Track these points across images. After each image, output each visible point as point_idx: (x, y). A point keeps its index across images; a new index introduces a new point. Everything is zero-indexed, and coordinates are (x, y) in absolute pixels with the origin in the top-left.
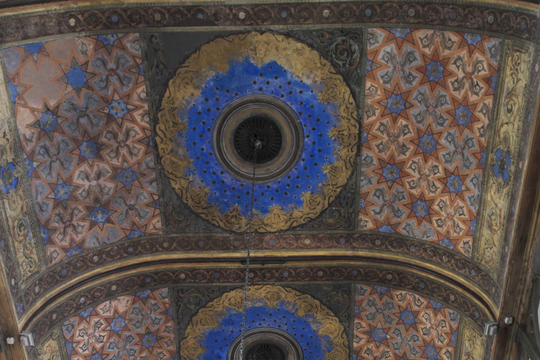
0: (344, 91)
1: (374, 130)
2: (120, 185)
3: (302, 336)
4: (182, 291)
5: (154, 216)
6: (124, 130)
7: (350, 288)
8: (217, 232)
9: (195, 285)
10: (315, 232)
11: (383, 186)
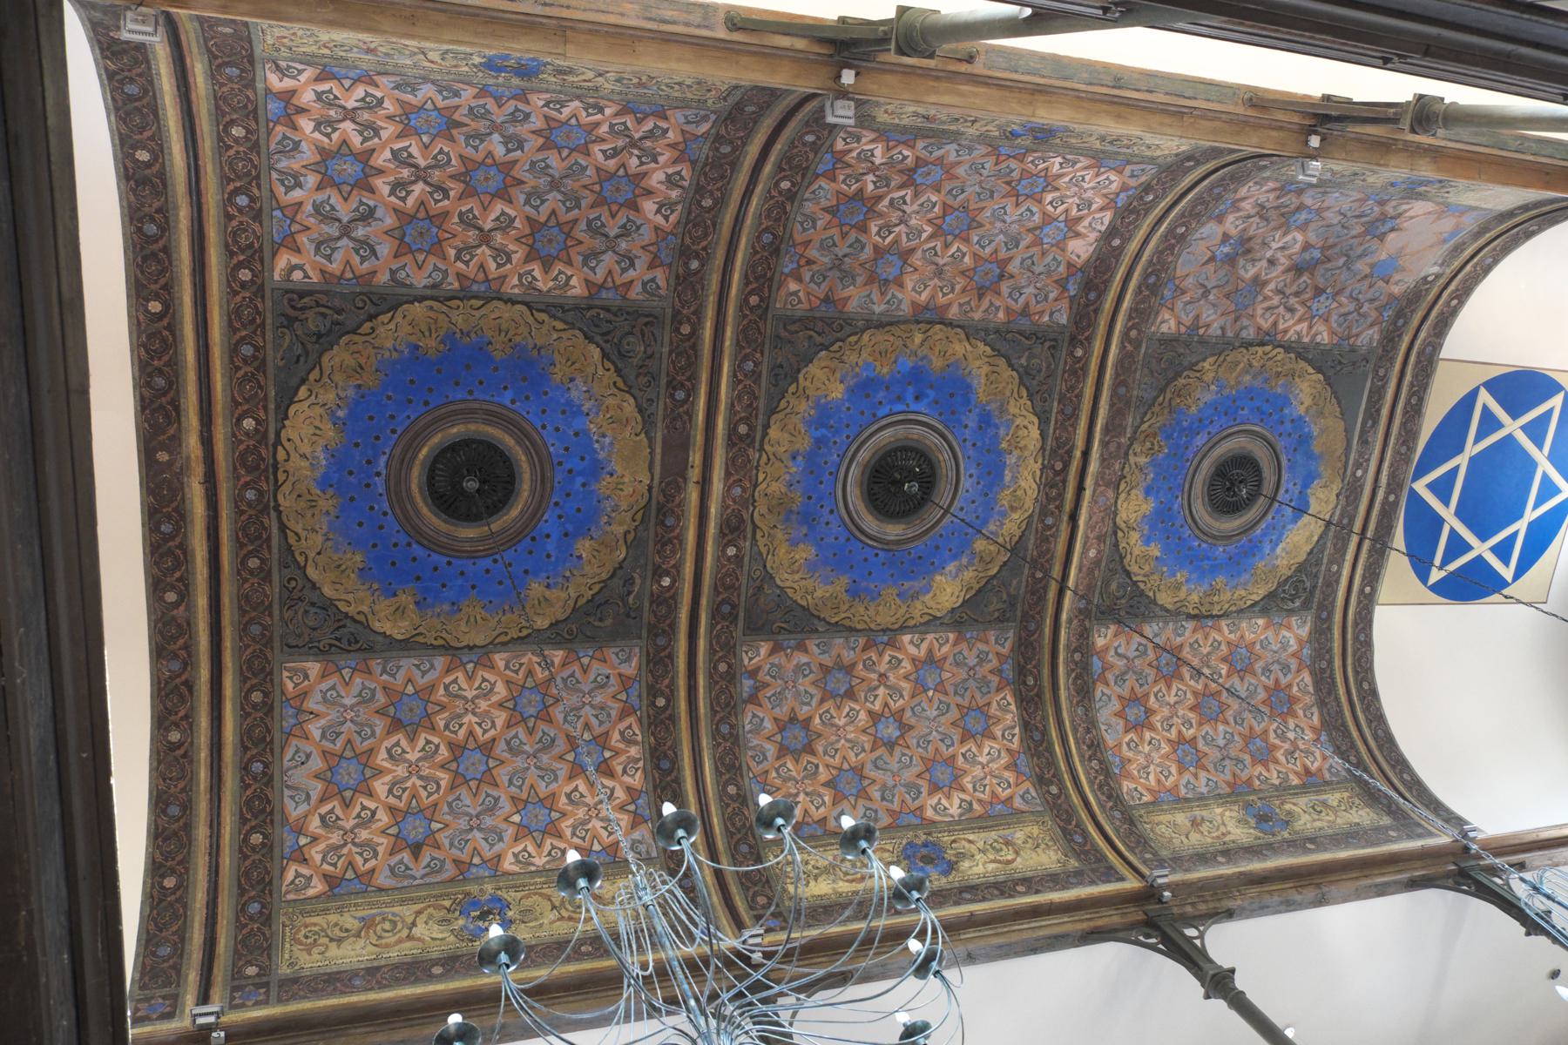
0: (1259, 592)
1: (1214, 635)
2: (1242, 285)
3: (937, 547)
4: (1054, 347)
7: (1008, 620)
9: (1060, 372)
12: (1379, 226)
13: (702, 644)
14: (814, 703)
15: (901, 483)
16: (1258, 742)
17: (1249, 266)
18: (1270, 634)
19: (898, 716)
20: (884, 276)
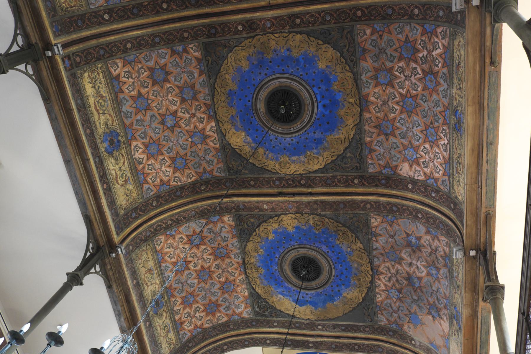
0: (259, 290)
1: (237, 273)
2: (398, 253)
3: (257, 130)
4: (357, 168)
5: (376, 227)
6: (392, 282)
7: (229, 172)
8: (330, 214)
9: (346, 174)
10: (261, 213)
11: (224, 244)
12: (434, 310)
13: (195, 22)
14: (176, 83)
15: (284, 106)
16: (192, 299)
17: (407, 254)
18: (242, 299)
19: (177, 125)
20: (379, 76)
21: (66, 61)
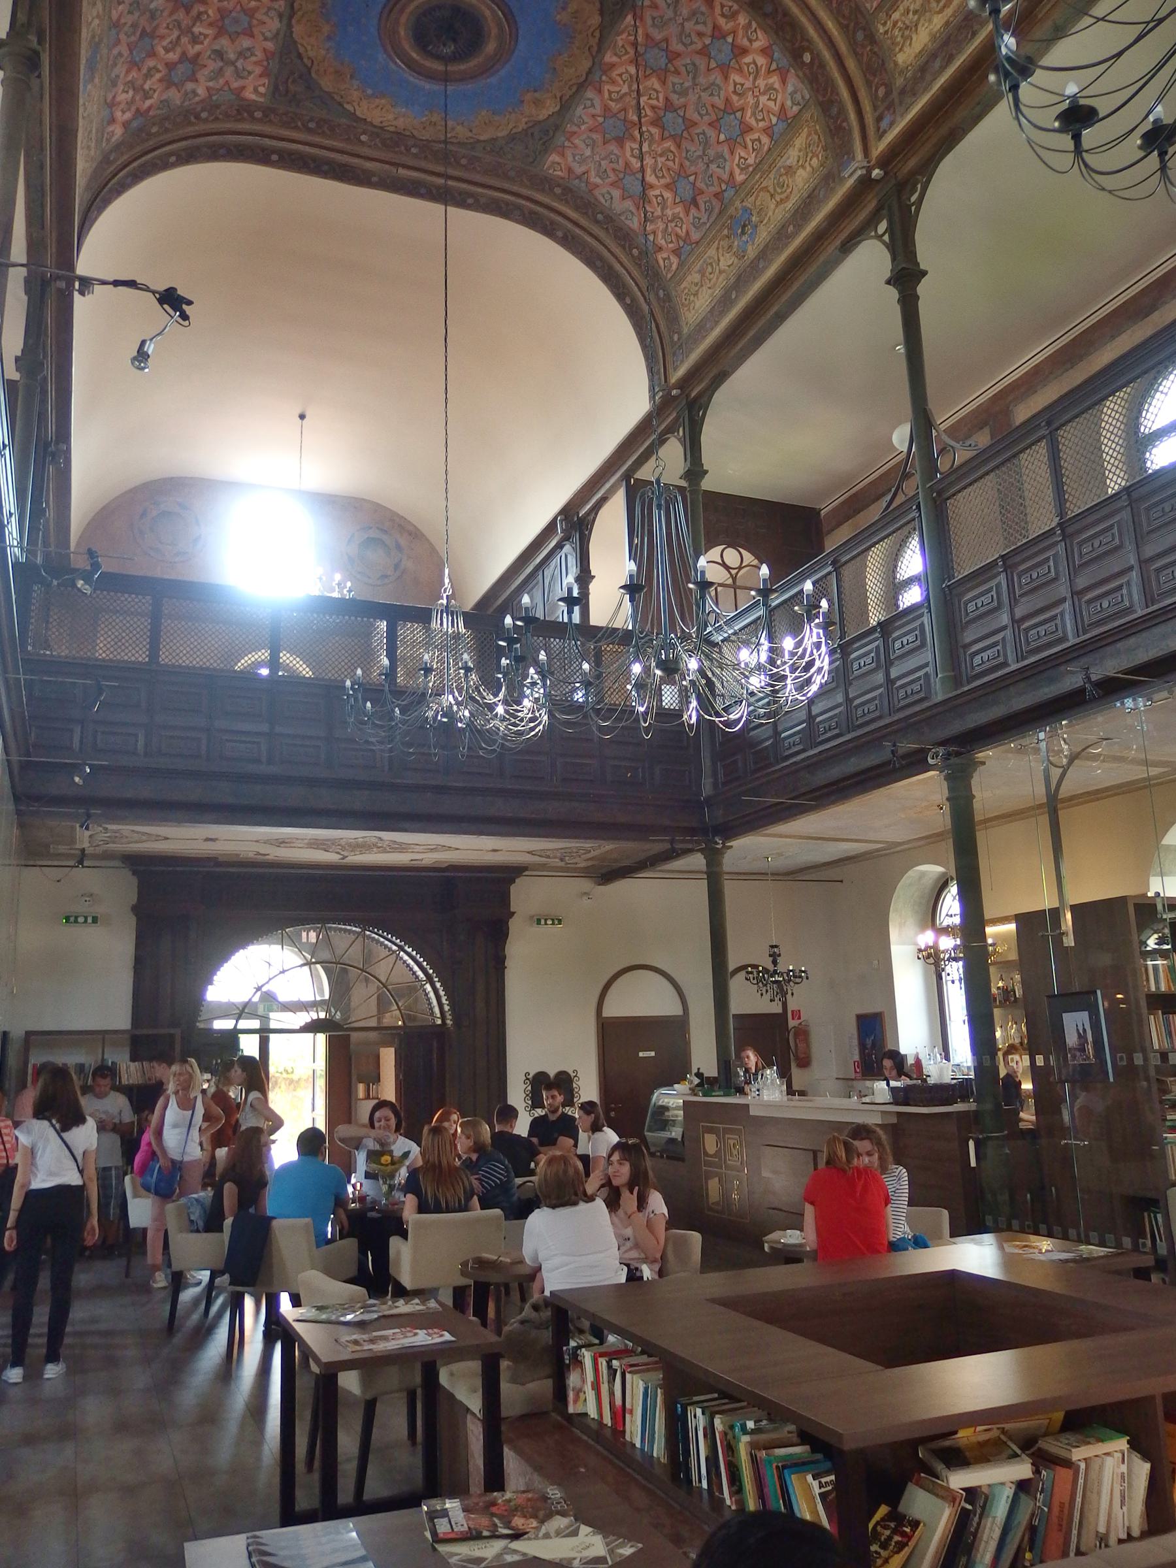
21: (884, 124)
